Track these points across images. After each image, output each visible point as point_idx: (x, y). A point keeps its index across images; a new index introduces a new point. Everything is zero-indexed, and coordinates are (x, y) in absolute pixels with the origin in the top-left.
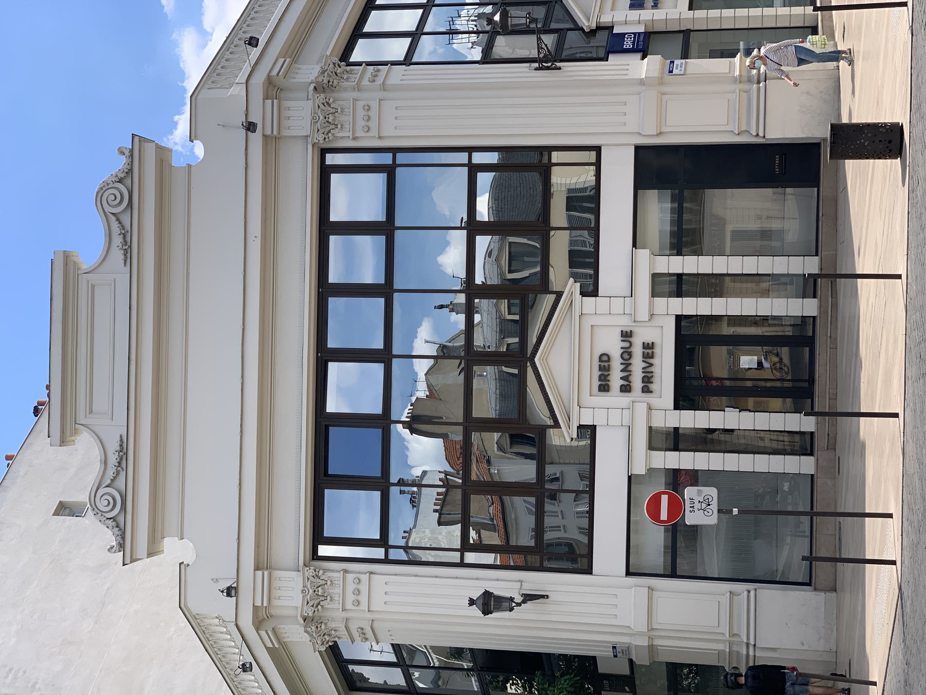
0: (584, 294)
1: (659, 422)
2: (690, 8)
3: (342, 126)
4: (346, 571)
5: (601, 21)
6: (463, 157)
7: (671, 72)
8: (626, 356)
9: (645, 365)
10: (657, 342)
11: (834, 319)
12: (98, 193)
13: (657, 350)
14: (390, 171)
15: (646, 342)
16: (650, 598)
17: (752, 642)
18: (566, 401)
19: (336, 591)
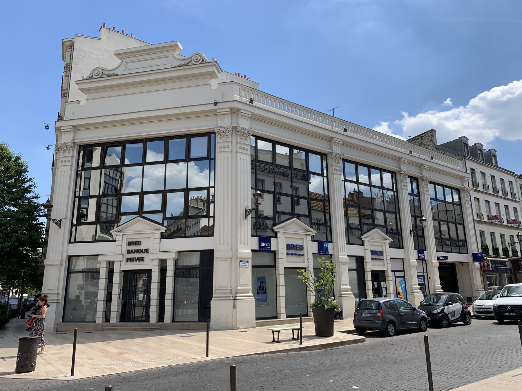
0: (162, 234)
1: (116, 265)
2: (285, 268)
3: (222, 138)
4: (72, 157)
5: (279, 233)
6: (212, 184)
7: (241, 261)
8: (140, 251)
9: (136, 258)
10: (144, 263)
11: (143, 329)
12: (199, 53)
13: (141, 262)
14: (208, 158)
15: (145, 259)
16: (57, 265)
17: (56, 301)
18: (124, 230)
19: (66, 154)
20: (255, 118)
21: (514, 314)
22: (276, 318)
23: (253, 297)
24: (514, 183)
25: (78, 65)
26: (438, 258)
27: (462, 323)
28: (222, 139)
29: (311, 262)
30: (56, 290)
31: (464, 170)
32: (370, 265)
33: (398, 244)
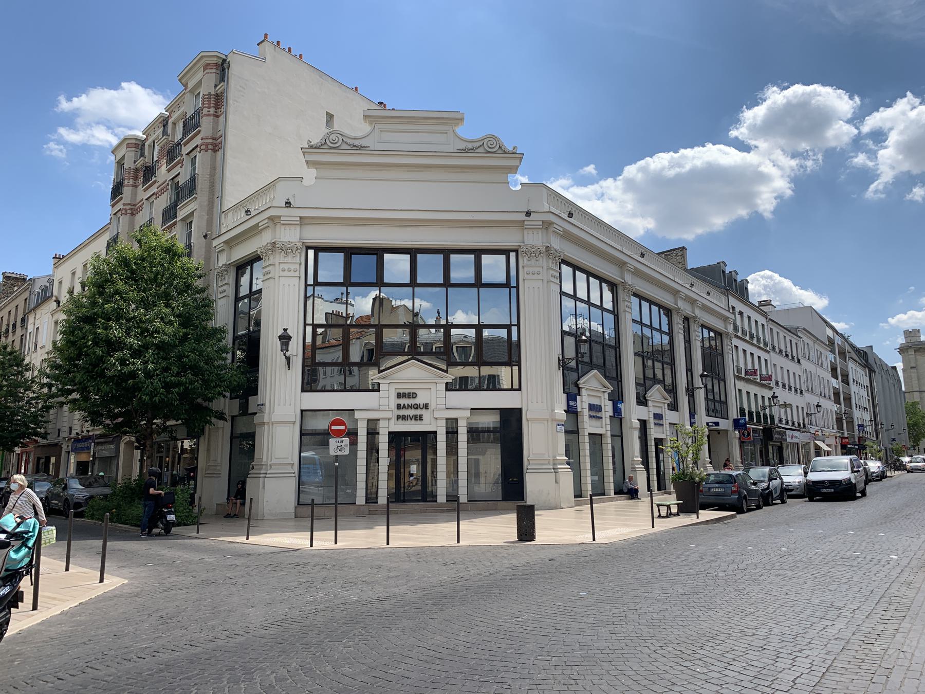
0: (447, 384)
1: (382, 424)
2: (589, 434)
4: (300, 264)
6: (514, 322)
7: (558, 425)
8: (416, 406)
9: (411, 417)
10: (423, 422)
13: (419, 422)
14: (507, 285)
16: (289, 422)
20: (566, 236)
21: (832, 490)
22: (604, 494)
23: (570, 470)
24: (766, 327)
25: (237, 102)
26: (707, 424)
27: (779, 501)
28: (530, 263)
29: (609, 428)
30: (290, 458)
31: (727, 309)
32: (654, 433)
33: (674, 407)
